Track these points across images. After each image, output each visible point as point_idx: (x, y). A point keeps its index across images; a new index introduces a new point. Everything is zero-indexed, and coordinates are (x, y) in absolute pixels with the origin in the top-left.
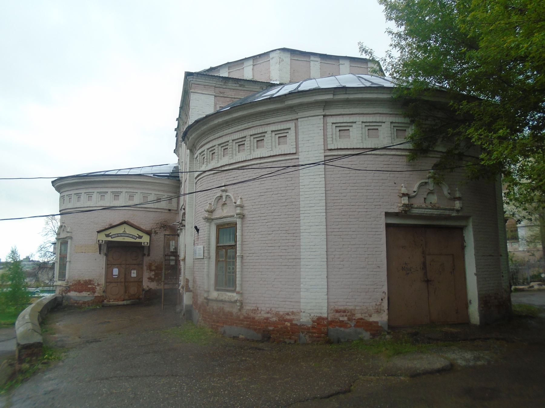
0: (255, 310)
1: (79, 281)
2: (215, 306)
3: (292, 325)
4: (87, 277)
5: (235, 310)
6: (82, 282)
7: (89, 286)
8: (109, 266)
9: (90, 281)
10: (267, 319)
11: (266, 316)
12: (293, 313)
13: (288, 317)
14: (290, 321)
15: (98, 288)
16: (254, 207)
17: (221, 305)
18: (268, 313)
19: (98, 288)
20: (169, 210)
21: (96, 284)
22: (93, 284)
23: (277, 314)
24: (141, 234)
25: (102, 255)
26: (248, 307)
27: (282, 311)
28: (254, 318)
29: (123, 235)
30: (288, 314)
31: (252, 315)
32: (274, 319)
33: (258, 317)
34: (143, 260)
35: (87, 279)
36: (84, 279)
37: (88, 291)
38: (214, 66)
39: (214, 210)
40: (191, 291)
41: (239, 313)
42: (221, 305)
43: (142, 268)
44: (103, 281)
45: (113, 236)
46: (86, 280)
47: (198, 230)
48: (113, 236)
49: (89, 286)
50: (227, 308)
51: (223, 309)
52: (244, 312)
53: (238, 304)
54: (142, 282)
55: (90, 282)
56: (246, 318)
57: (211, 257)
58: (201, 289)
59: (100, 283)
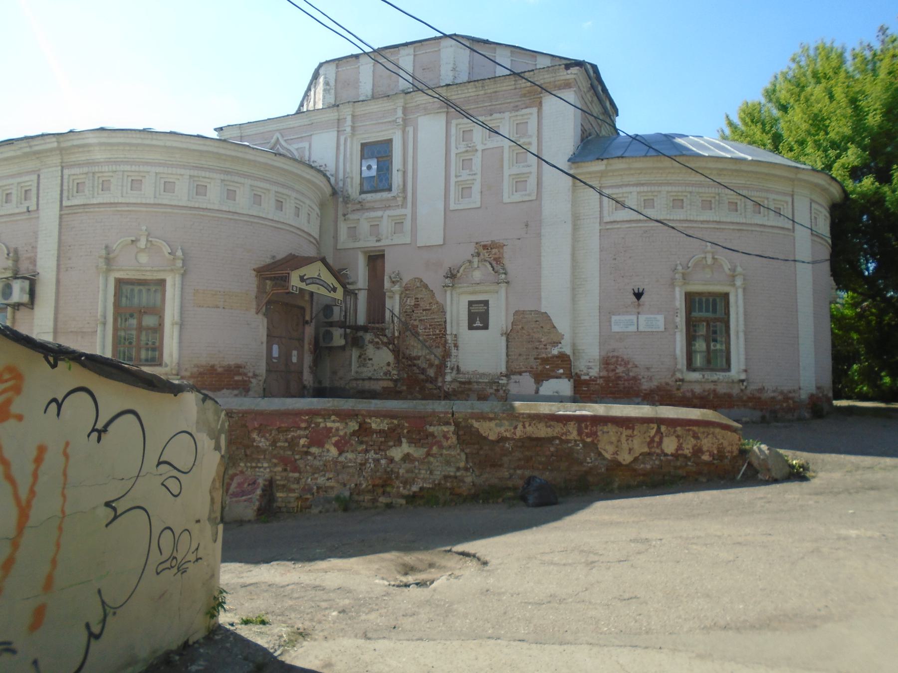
0: (762, 390)
1: (213, 367)
2: (698, 389)
3: (794, 402)
4: (231, 361)
5: (735, 391)
6: (220, 370)
7: (236, 378)
8: (271, 337)
9: (239, 367)
10: (773, 398)
11: (772, 395)
12: (794, 391)
13: (791, 395)
14: (792, 398)
15: (253, 380)
18: (774, 391)
19: (253, 380)
21: (250, 374)
22: (245, 374)
23: (782, 393)
24: (337, 285)
25: (260, 316)
26: (752, 387)
27: (786, 389)
28: (760, 398)
29: (318, 281)
30: (790, 392)
31: (758, 395)
32: (780, 397)
33: (765, 396)
34: (304, 333)
35: (232, 363)
36: (225, 363)
37: (234, 389)
38: (491, 40)
42: (712, 387)
43: (303, 347)
44: (262, 369)
45: (308, 282)
46: (229, 366)
47: (638, 295)
48: (308, 282)
49: (236, 378)
50: (722, 389)
51: (714, 391)
52: (748, 392)
53: (745, 384)
54: (301, 373)
55: (237, 369)
56: (749, 398)
58: (652, 370)
59: (257, 372)
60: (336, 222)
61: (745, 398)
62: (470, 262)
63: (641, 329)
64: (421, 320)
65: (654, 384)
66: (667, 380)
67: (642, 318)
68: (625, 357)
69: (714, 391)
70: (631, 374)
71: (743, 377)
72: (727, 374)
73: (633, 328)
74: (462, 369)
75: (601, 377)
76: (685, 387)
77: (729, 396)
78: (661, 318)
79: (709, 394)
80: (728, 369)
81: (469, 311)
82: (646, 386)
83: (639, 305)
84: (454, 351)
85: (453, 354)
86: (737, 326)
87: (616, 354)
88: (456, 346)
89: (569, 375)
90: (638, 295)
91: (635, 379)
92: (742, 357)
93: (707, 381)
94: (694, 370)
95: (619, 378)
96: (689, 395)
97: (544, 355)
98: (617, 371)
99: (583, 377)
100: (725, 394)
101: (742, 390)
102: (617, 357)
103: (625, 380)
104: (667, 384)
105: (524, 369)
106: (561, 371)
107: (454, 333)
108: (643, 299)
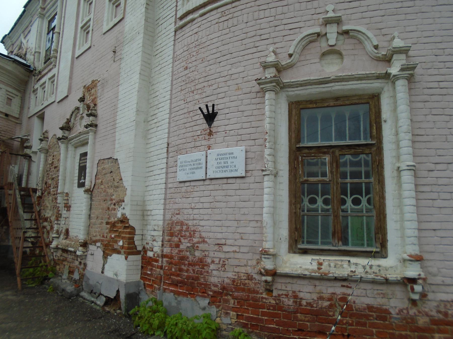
2: (307, 293)
5: (396, 302)
16: (440, 58)
17: (339, 290)
20: (7, 115)
39: (290, 66)
40: (138, 253)
41: (412, 312)
42: (339, 290)
47: (210, 117)
50: (361, 298)
51: (344, 299)
52: (430, 307)
53: (418, 288)
56: (434, 322)
57: (281, 173)
58: (226, 249)
60: (30, 94)
61: (422, 321)
62: (78, 109)
63: (211, 175)
64: (53, 179)
65: (227, 276)
66: (249, 270)
67: (213, 153)
68: (190, 223)
69: (344, 299)
70: (197, 254)
71: (413, 271)
72: (375, 262)
73: (200, 174)
74: (71, 234)
75: (163, 256)
76: (280, 287)
77: (383, 314)
78: (239, 152)
79: (331, 306)
80: (382, 253)
81: (80, 164)
82: (216, 277)
83: (211, 134)
84: (64, 213)
85: (63, 216)
86: (398, 158)
87: (180, 217)
88: (68, 207)
89: (131, 250)
90: (210, 117)
91: (202, 263)
92: (411, 229)
93: (324, 278)
94: (305, 252)
95: (183, 258)
96: (289, 302)
97: (112, 220)
98: (182, 247)
99: (150, 254)
100: (370, 308)
101: (414, 302)
102: (182, 224)
103: (190, 264)
104: (250, 278)
105: (98, 238)
106: (121, 243)
107: (66, 191)
108: (215, 124)
